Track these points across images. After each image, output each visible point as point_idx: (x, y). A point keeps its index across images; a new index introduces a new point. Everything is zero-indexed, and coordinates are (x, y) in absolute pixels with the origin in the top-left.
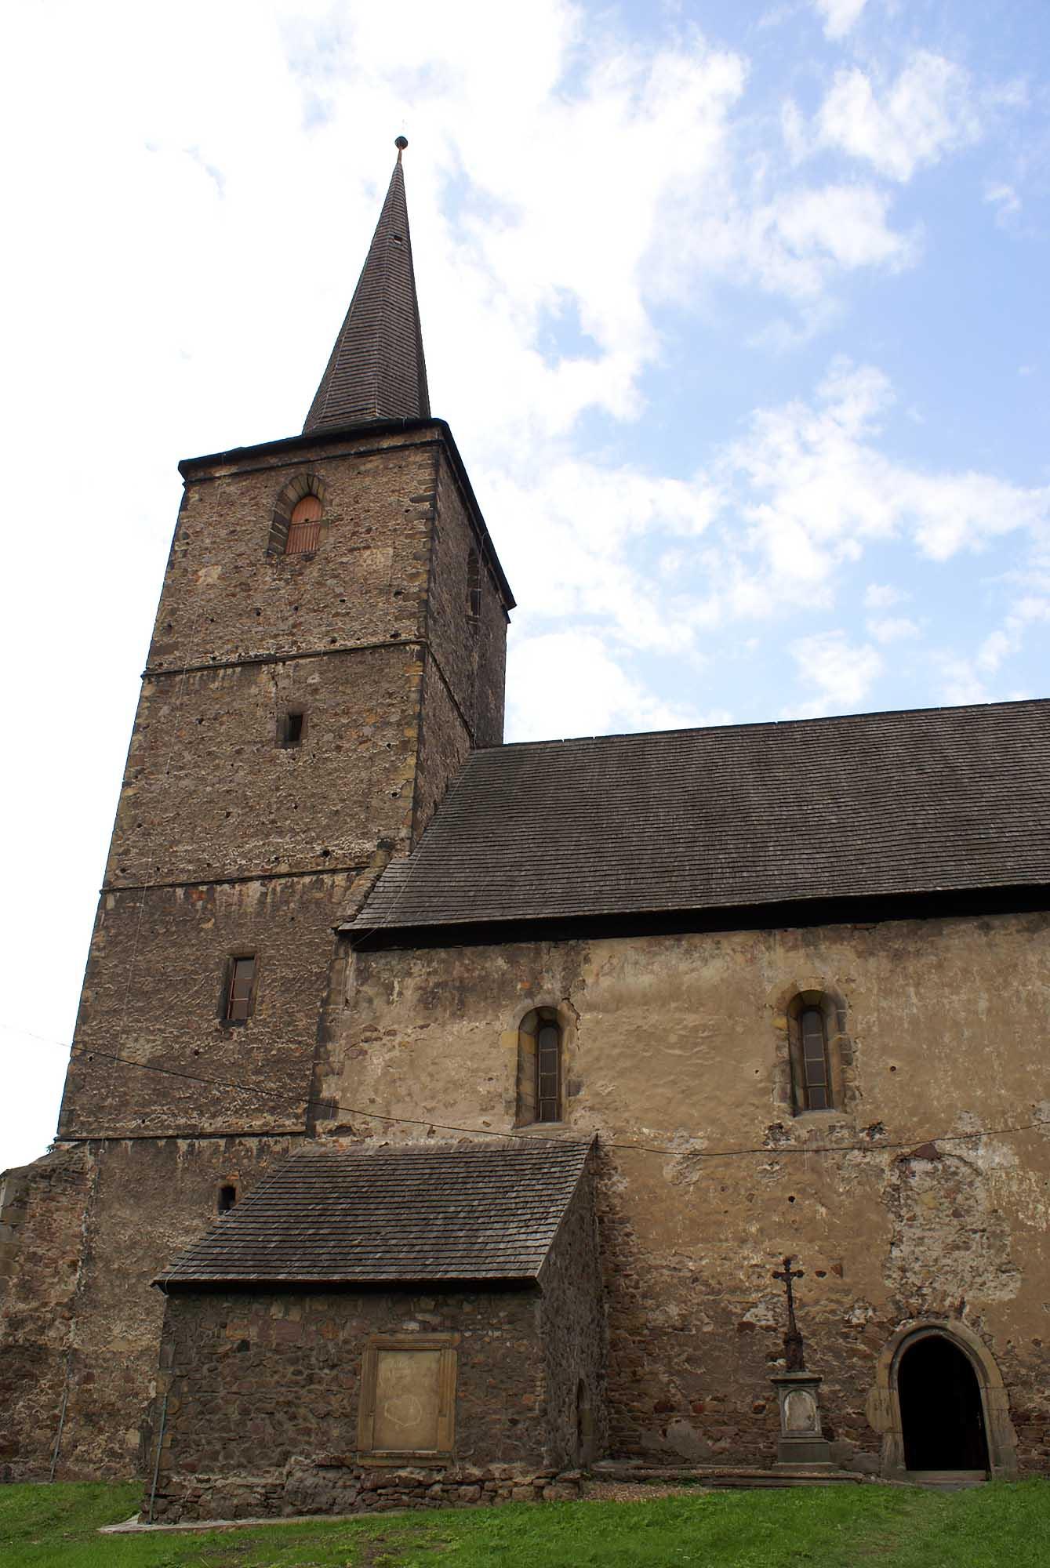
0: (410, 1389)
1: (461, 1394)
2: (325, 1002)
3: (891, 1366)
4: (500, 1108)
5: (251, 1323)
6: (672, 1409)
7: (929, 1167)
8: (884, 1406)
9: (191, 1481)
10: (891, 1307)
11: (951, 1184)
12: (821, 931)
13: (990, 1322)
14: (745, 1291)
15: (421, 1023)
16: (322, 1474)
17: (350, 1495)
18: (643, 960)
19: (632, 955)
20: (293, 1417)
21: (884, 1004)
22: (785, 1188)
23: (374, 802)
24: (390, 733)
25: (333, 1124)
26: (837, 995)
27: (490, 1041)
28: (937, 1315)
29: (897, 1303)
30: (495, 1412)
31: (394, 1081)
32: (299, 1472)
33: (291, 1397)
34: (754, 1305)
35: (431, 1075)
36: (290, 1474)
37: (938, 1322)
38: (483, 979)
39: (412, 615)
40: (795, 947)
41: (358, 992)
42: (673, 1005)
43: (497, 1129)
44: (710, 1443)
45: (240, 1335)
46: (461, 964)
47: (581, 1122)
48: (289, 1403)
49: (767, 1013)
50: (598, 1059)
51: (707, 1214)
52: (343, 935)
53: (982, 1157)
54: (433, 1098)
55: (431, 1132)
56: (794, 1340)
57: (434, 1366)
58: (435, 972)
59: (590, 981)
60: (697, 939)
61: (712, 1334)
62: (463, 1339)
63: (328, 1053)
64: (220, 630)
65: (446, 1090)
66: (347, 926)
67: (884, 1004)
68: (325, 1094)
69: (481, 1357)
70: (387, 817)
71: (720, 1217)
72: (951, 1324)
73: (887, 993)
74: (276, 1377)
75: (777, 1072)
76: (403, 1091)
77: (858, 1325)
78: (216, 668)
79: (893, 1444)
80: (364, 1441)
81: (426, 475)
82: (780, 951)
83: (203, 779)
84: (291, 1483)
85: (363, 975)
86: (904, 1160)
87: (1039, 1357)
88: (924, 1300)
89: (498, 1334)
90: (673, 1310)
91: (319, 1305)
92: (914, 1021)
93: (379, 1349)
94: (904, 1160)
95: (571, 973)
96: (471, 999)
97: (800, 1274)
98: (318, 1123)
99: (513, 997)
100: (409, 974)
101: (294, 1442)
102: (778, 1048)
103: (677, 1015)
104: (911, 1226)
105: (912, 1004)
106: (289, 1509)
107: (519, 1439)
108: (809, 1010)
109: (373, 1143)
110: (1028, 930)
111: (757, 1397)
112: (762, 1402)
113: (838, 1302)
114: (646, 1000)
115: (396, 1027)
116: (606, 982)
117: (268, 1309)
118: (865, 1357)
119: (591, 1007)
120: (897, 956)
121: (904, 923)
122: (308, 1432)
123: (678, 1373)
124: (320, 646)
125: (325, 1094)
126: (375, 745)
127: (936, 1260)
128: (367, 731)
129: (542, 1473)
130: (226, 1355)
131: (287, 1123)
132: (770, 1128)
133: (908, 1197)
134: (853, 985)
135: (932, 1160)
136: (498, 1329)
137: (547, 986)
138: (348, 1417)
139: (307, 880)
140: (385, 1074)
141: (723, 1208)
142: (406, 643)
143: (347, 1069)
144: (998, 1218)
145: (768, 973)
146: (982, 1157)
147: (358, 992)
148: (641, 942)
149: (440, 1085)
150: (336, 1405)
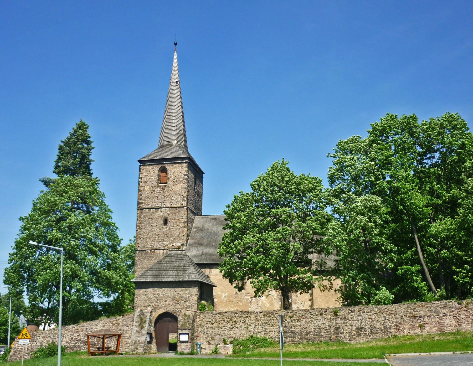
24: (182, 224)
39: (185, 201)
64: (150, 200)
78: (151, 209)
81: (186, 169)
83: (150, 230)
86: (252, 298)
94: (252, 298)
124: (169, 206)
128: (178, 223)
142: (183, 207)
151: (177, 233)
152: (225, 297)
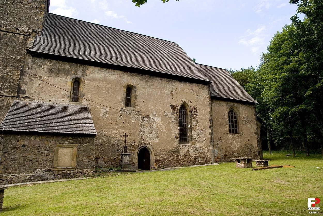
0: (66, 155)
1: (77, 156)
2: (23, 67)
3: (138, 152)
4: (66, 97)
5: (26, 141)
6: (99, 159)
7: (147, 119)
8: (136, 158)
9: (9, 176)
10: (139, 142)
11: (150, 123)
12: (134, 74)
13: (154, 146)
14: (114, 138)
15: (48, 76)
16: (44, 172)
17: (52, 176)
18: (99, 72)
19: (97, 71)
20: (37, 161)
21: (143, 90)
22: (123, 120)
23: (32, 20)
24: (37, 4)
25: (24, 96)
26: (135, 87)
27: (66, 82)
28: (146, 144)
29: (140, 142)
30: (85, 160)
31: (41, 88)
32: (39, 172)
33: (37, 157)
34: (115, 141)
35: (50, 88)
36: (37, 173)
37: (146, 145)
38: (64, 69)
40: (129, 76)
41: (32, 66)
42: (105, 82)
43: (66, 103)
44: (106, 165)
45: (22, 143)
46: (59, 65)
47: (84, 103)
48: (36, 158)
49: (122, 87)
50: (88, 91)
51: (108, 124)
52: (28, 52)
53: (156, 119)
54: (50, 93)
55: (50, 101)
56: (125, 147)
57: (71, 150)
58: (52, 65)
59: (88, 74)
60: (110, 70)
61: (107, 145)
62: (78, 145)
63: (23, 79)
65: (54, 92)
66: (30, 50)
67: (143, 90)
68: (22, 88)
69: (82, 149)
70: (35, 25)
71: (111, 124)
72: (148, 146)
73: (144, 88)
74: (33, 153)
75: (123, 99)
76: (43, 91)
77: (133, 145)
79: (137, 165)
80: (55, 165)
82: (126, 76)
84: (37, 175)
85: (33, 62)
86: (143, 118)
87: (160, 151)
88: (144, 142)
89: (85, 145)
90: (100, 141)
91: (44, 138)
92: (148, 94)
93: (59, 147)
94: (143, 118)
95: (84, 72)
96: (61, 73)
97: (128, 136)
98: (20, 95)
99: (71, 74)
100: (46, 64)
101: (37, 166)
102: (124, 94)
103: (105, 84)
104: (143, 129)
105: (148, 91)
106: (37, 180)
107: (90, 165)
108: (130, 89)
109: (35, 102)
110: (168, 82)
111: (114, 157)
112: (115, 158)
113: (130, 141)
114: (99, 80)
115: (42, 76)
116: (91, 75)
117: (30, 138)
118: (134, 151)
119: (88, 80)
120: (146, 82)
121: (148, 76)
122: (41, 164)
123: (101, 152)
125: (22, 88)
126: (32, 5)
127: (147, 135)
129: (94, 171)
130: (19, 148)
131: (4, 93)
132: (121, 109)
133: (143, 124)
134: (138, 85)
135: (148, 118)
136: (86, 144)
137: (79, 73)
138: (51, 161)
139: (11, 34)
140: (39, 86)
141: (111, 123)
143: (29, 83)
144: (157, 129)
145: (123, 80)
146: (156, 119)
147: (32, 66)
148: (99, 68)
149: (53, 91)
150: (49, 159)
151: (26, 13)
152: (106, 113)
